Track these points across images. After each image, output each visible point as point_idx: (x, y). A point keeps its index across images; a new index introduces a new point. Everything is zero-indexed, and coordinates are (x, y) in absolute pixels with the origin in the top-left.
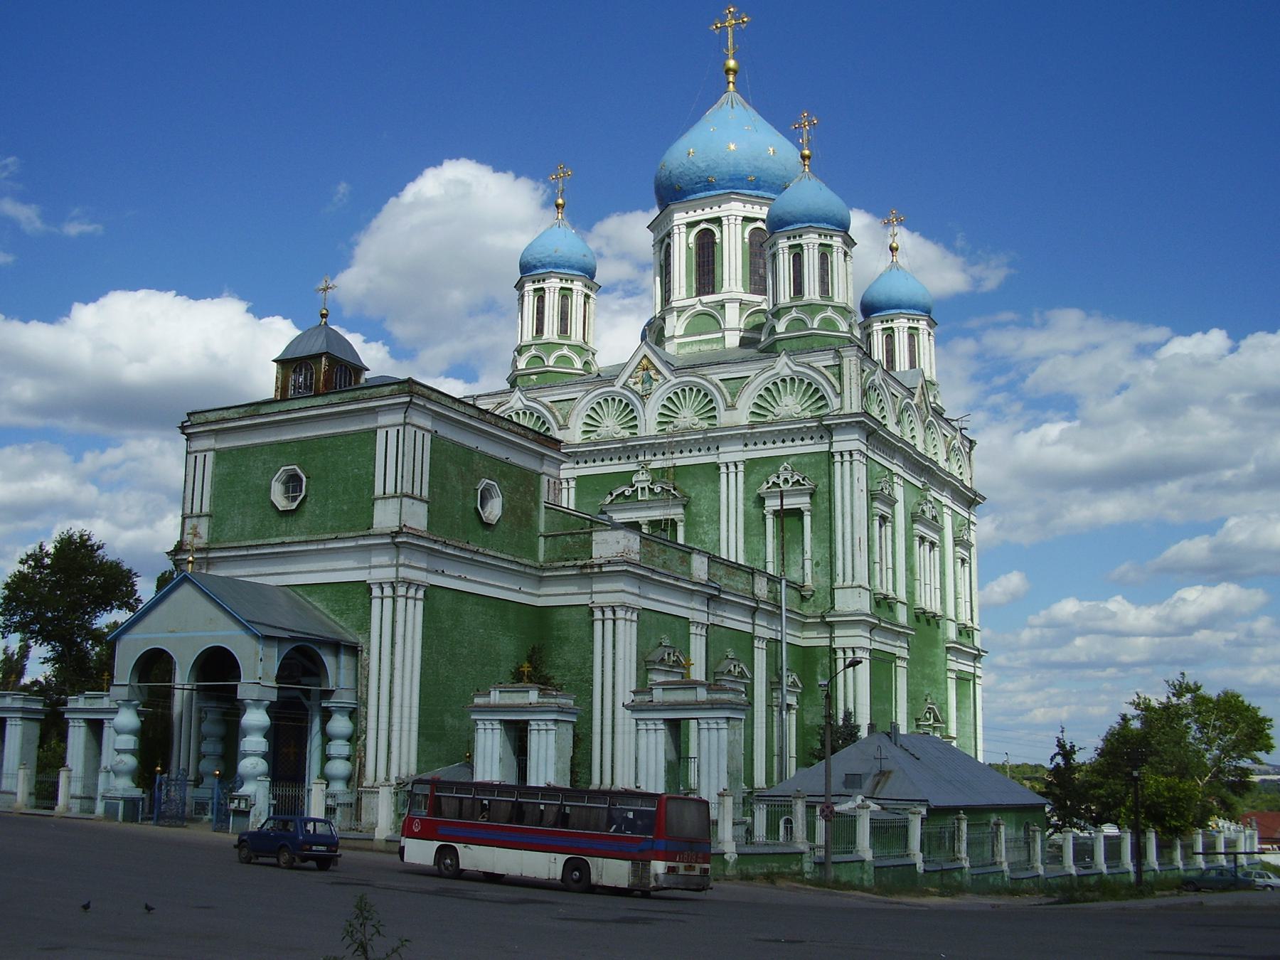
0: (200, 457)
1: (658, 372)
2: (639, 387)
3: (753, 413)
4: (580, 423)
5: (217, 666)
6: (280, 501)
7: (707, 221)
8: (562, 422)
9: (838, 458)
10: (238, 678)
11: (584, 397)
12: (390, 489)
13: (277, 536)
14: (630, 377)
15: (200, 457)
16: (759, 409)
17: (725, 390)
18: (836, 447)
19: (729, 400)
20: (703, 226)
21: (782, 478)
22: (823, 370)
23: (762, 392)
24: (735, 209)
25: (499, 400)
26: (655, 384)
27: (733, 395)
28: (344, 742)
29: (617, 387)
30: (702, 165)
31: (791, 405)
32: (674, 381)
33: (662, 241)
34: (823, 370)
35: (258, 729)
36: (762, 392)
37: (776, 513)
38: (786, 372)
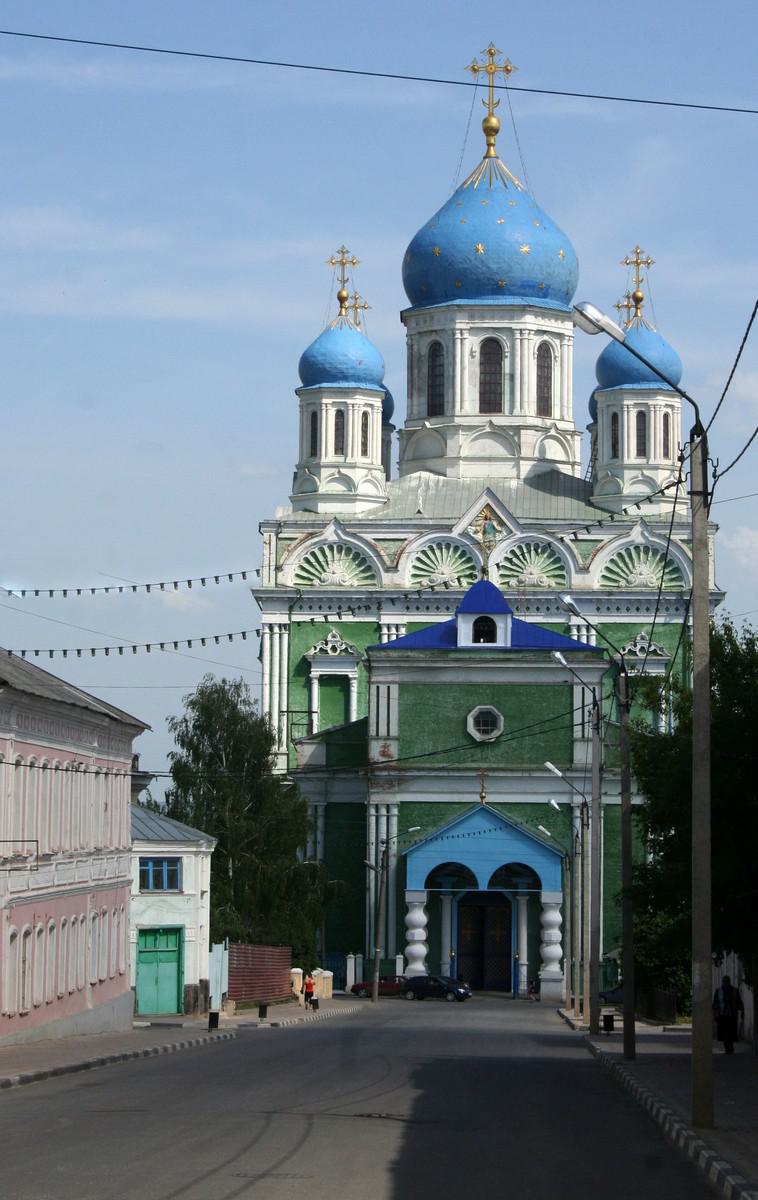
0: (383, 689)
1: (502, 523)
2: (479, 537)
3: (603, 576)
4: (410, 566)
6: (478, 736)
8: (388, 563)
11: (416, 539)
13: (473, 761)
15: (383, 689)
16: (610, 574)
17: (576, 551)
19: (580, 561)
21: (639, 647)
22: (680, 543)
23: (615, 558)
25: (310, 530)
27: (585, 557)
29: (455, 533)
30: (494, 266)
31: (647, 574)
32: (519, 535)
34: (680, 543)
36: (615, 558)
38: (640, 540)
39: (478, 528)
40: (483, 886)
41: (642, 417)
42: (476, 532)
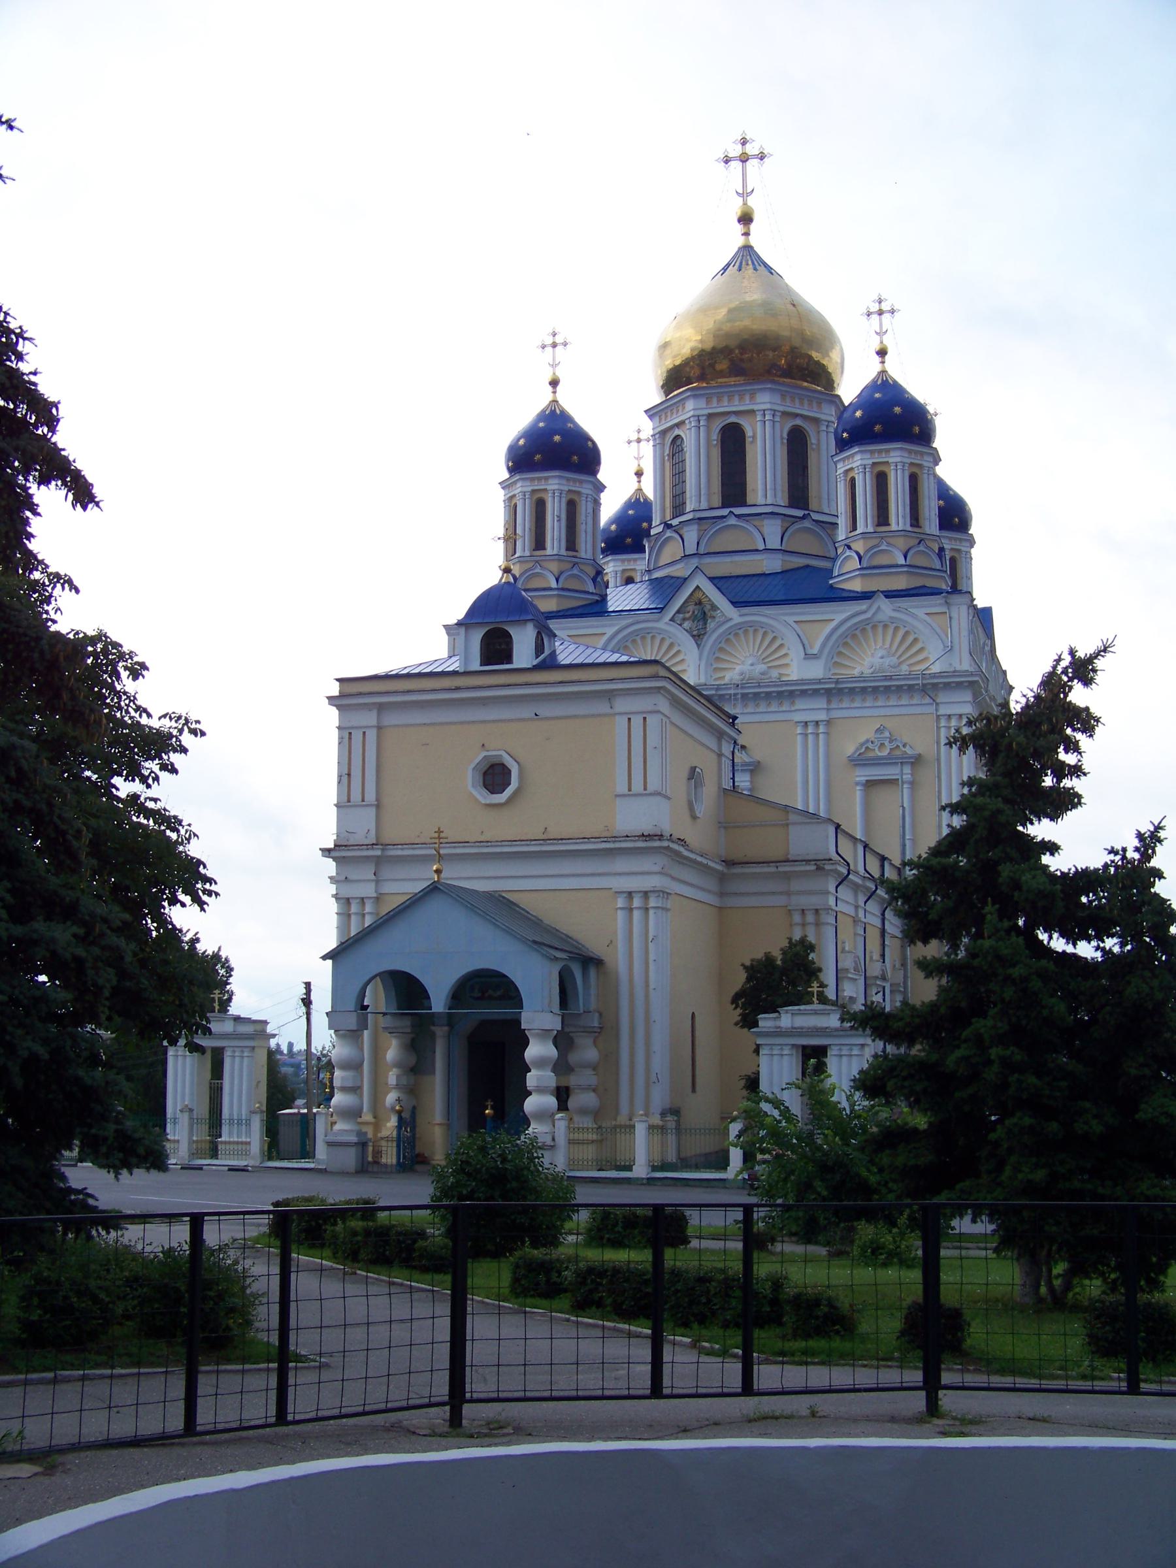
1: (714, 607)
5: (487, 988)
7: (735, 413)
9: (943, 723)
10: (522, 1008)
12: (637, 786)
14: (678, 612)
18: (942, 711)
20: (733, 419)
24: (765, 400)
26: (711, 625)
28: (589, 1072)
33: (663, 433)
35: (541, 1063)
37: (870, 785)
38: (880, 617)
39: (687, 615)
40: (439, 1003)
41: (881, 480)
42: (684, 619)
